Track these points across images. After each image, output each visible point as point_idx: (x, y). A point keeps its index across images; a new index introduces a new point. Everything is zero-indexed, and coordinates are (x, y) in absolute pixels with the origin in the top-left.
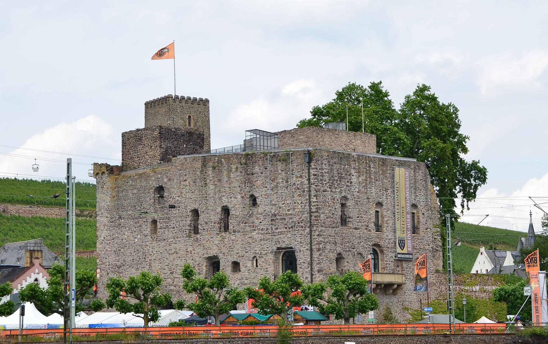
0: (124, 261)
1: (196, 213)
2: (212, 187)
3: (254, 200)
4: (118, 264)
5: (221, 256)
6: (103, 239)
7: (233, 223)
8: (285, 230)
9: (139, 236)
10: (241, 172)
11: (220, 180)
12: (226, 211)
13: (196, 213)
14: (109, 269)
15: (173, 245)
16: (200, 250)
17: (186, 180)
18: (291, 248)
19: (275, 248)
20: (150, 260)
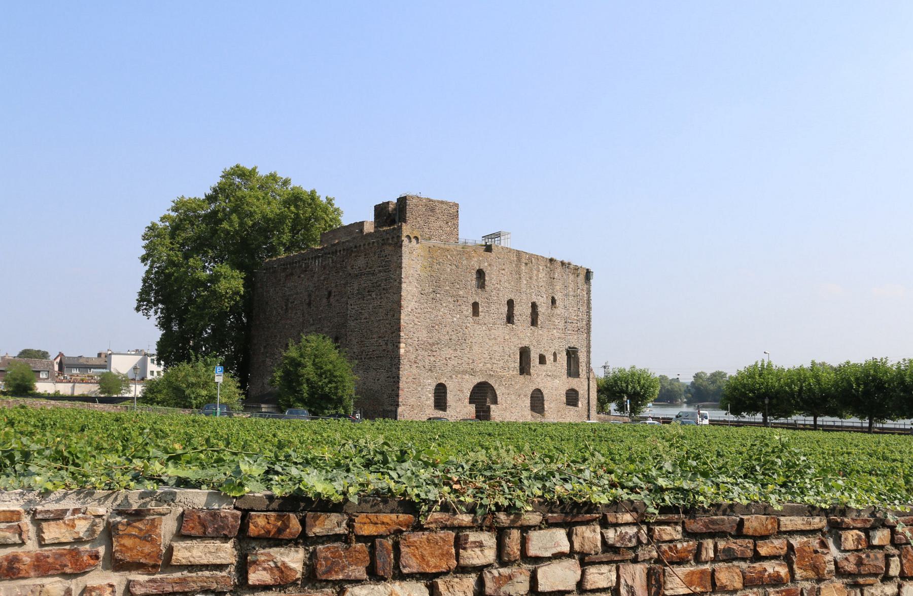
0: (439, 339)
1: (510, 303)
2: (525, 282)
3: (553, 301)
4: (431, 341)
5: (532, 348)
6: (410, 310)
7: (541, 319)
8: (573, 332)
9: (458, 316)
10: (546, 274)
11: (530, 278)
12: (534, 306)
13: (510, 303)
14: (418, 346)
15: (493, 331)
16: (515, 340)
17: (504, 269)
18: (576, 348)
19: (567, 347)
20: (471, 342)
